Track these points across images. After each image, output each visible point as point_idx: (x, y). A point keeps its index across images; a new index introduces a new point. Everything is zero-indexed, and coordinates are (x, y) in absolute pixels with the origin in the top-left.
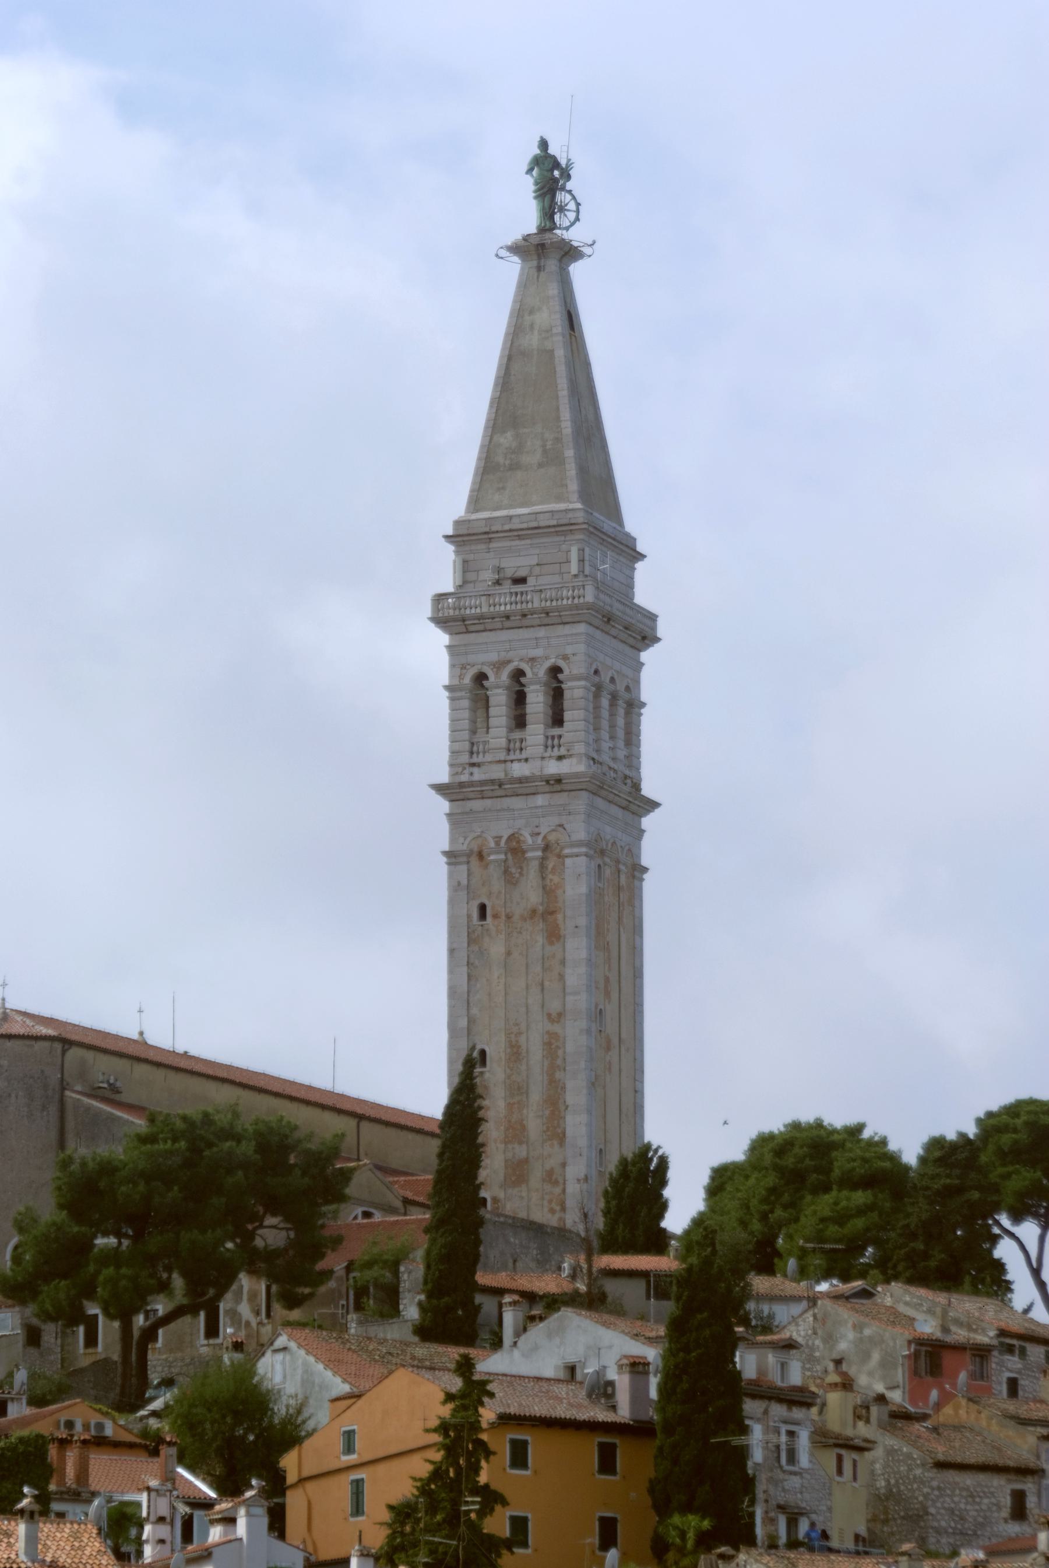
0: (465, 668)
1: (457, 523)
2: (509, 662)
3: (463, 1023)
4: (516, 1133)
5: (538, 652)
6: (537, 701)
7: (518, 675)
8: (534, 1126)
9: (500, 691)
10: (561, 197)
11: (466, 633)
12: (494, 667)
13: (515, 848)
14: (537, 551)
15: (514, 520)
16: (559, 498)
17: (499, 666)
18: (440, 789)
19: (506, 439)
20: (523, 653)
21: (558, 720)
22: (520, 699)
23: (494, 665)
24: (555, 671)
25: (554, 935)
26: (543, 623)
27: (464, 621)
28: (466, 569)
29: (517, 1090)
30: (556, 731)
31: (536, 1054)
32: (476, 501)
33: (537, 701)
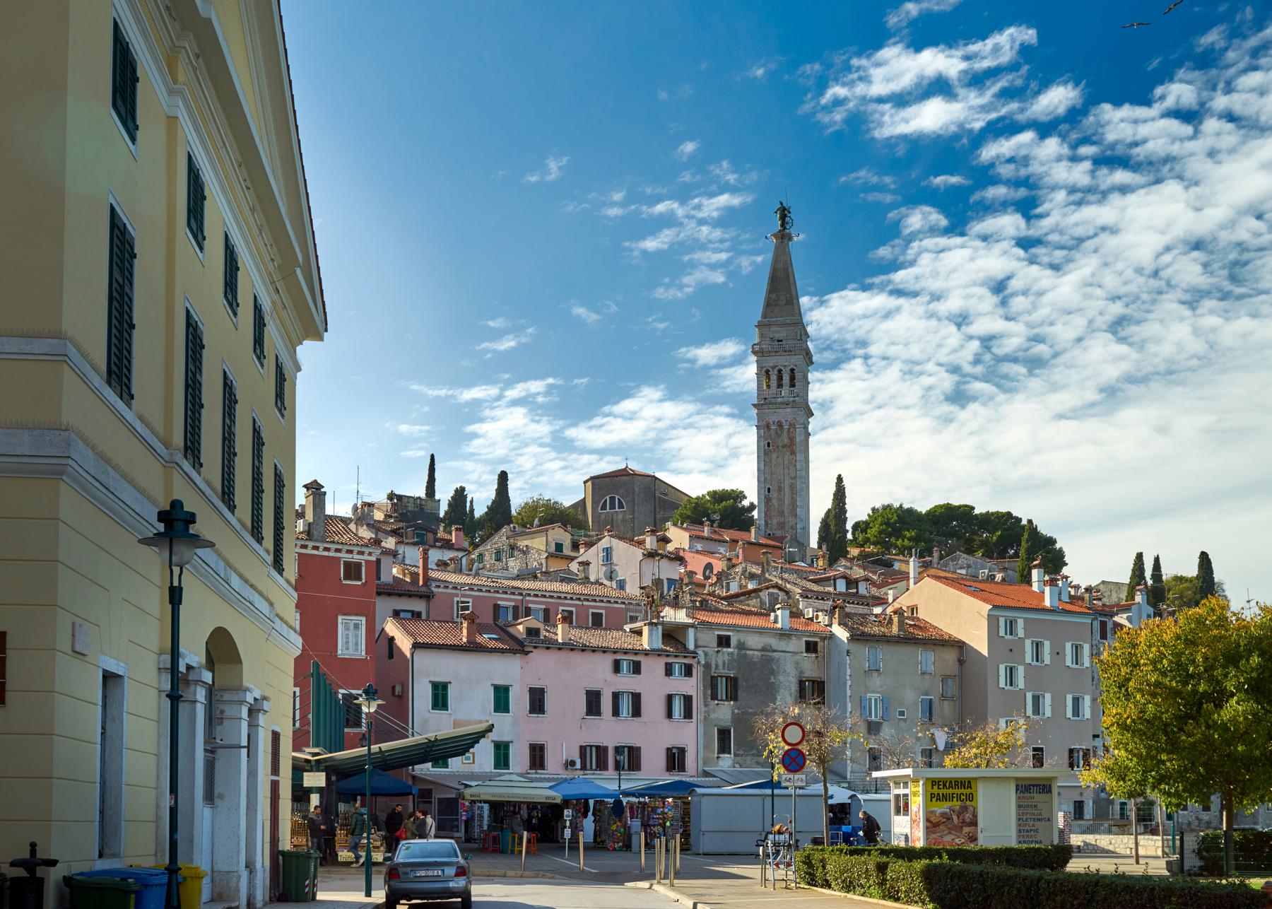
1: (759, 322)
3: (763, 479)
4: (782, 513)
5: (787, 364)
6: (786, 378)
7: (780, 371)
8: (786, 511)
10: (787, 219)
13: (780, 425)
16: (792, 315)
17: (773, 368)
18: (755, 405)
19: (773, 296)
21: (793, 385)
22: (780, 378)
24: (792, 370)
25: (793, 453)
28: (762, 335)
29: (781, 500)
30: (792, 389)
31: (787, 489)
32: (764, 315)
33: (786, 378)
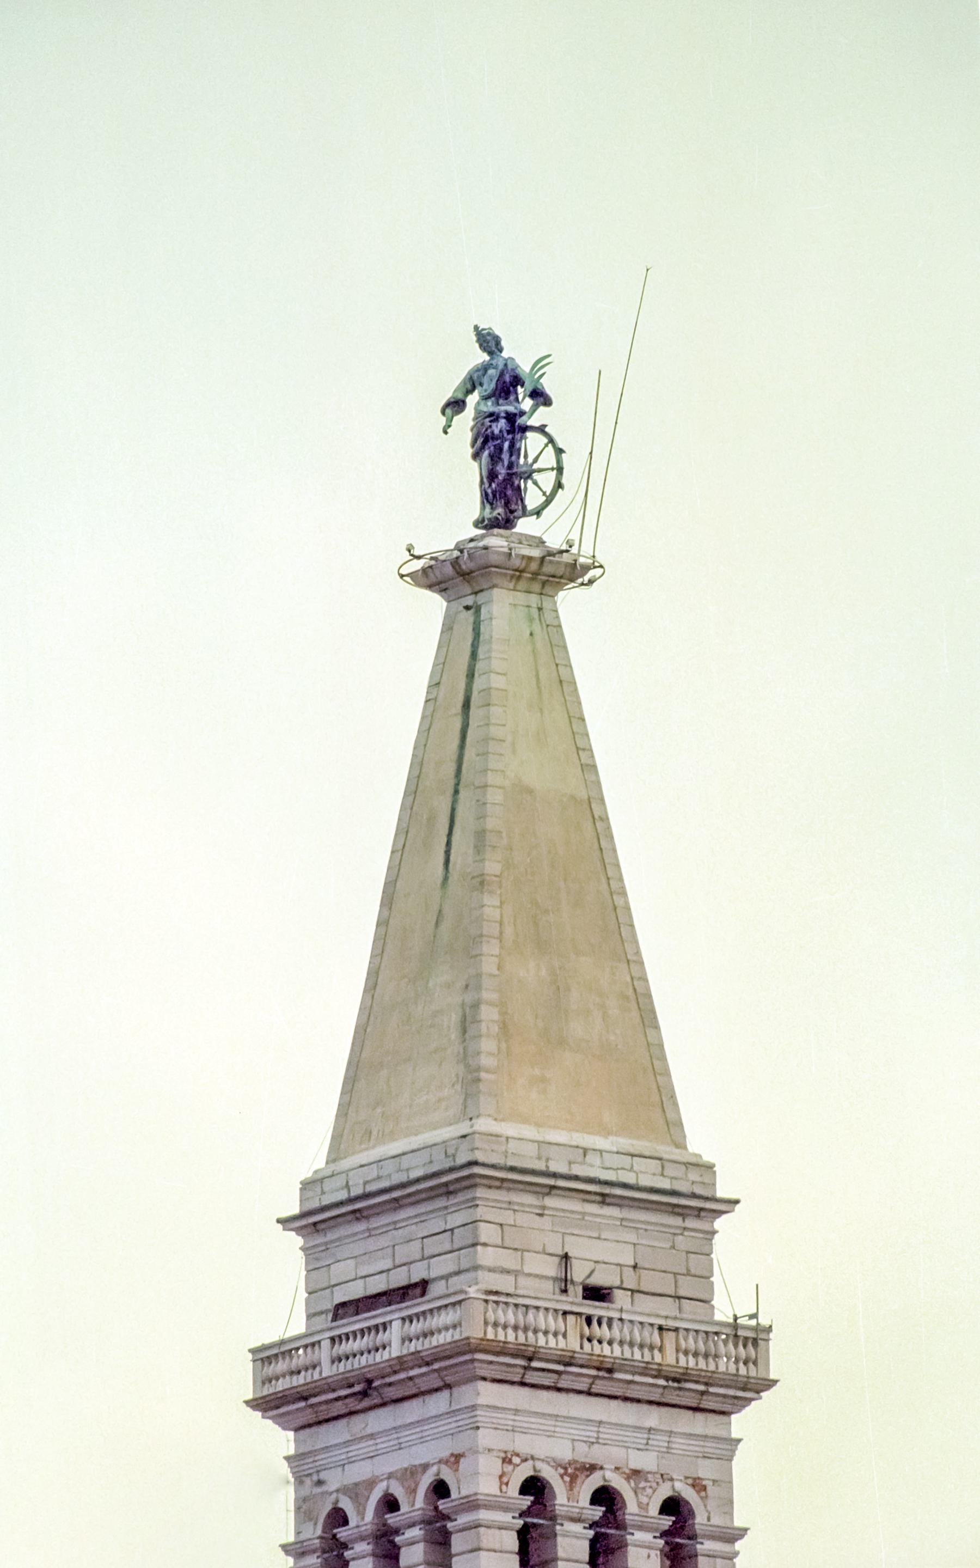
0: (510, 1462)
2: (592, 1468)
5: (645, 1461)
9: (577, 1528)
12: (566, 1473)
14: (631, 1237)
15: (592, 1158)
20: (617, 1454)
23: (566, 1469)
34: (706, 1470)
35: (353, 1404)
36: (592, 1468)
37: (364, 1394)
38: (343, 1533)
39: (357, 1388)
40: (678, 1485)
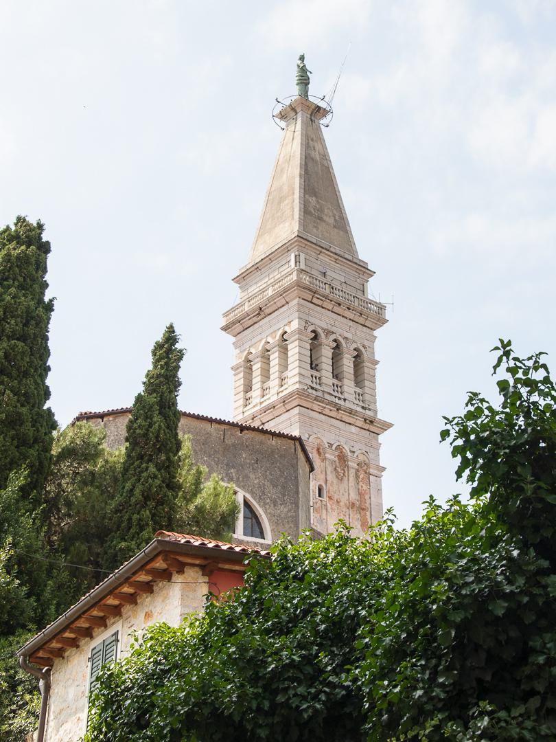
2: (333, 333)
6: (347, 364)
11: (308, 301)
26: (354, 320)
27: (315, 293)
33: (347, 364)
34: (366, 343)
35: (255, 319)
36: (333, 333)
37: (259, 314)
38: (250, 357)
39: (257, 312)
40: (359, 345)
